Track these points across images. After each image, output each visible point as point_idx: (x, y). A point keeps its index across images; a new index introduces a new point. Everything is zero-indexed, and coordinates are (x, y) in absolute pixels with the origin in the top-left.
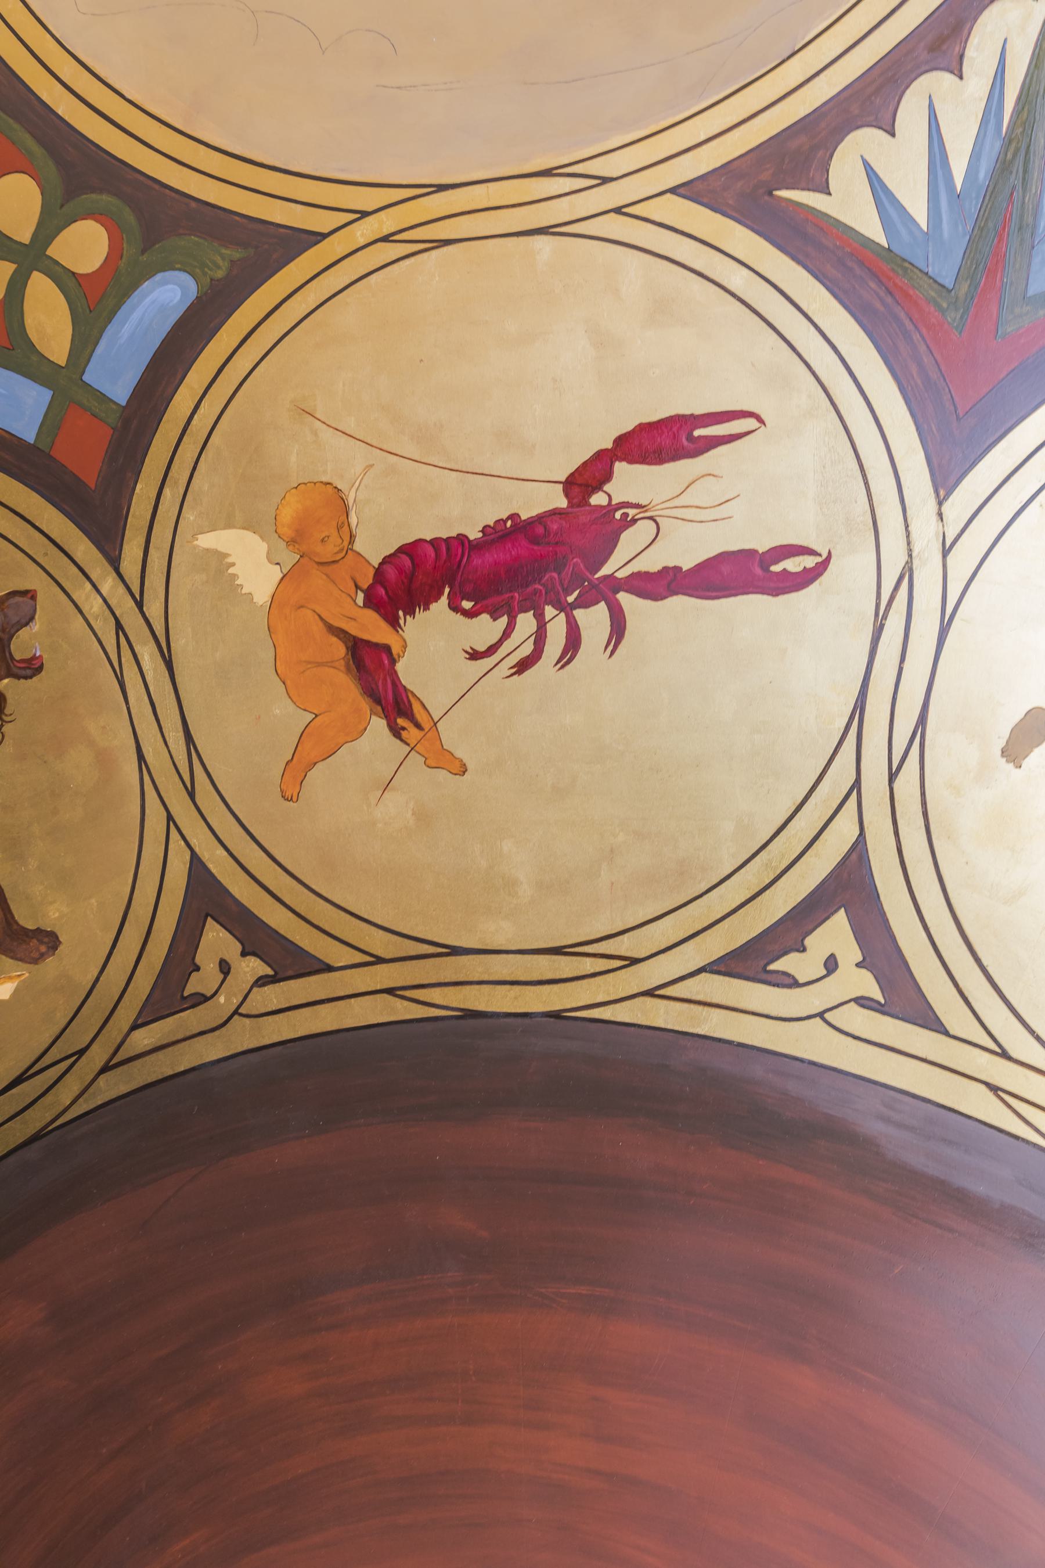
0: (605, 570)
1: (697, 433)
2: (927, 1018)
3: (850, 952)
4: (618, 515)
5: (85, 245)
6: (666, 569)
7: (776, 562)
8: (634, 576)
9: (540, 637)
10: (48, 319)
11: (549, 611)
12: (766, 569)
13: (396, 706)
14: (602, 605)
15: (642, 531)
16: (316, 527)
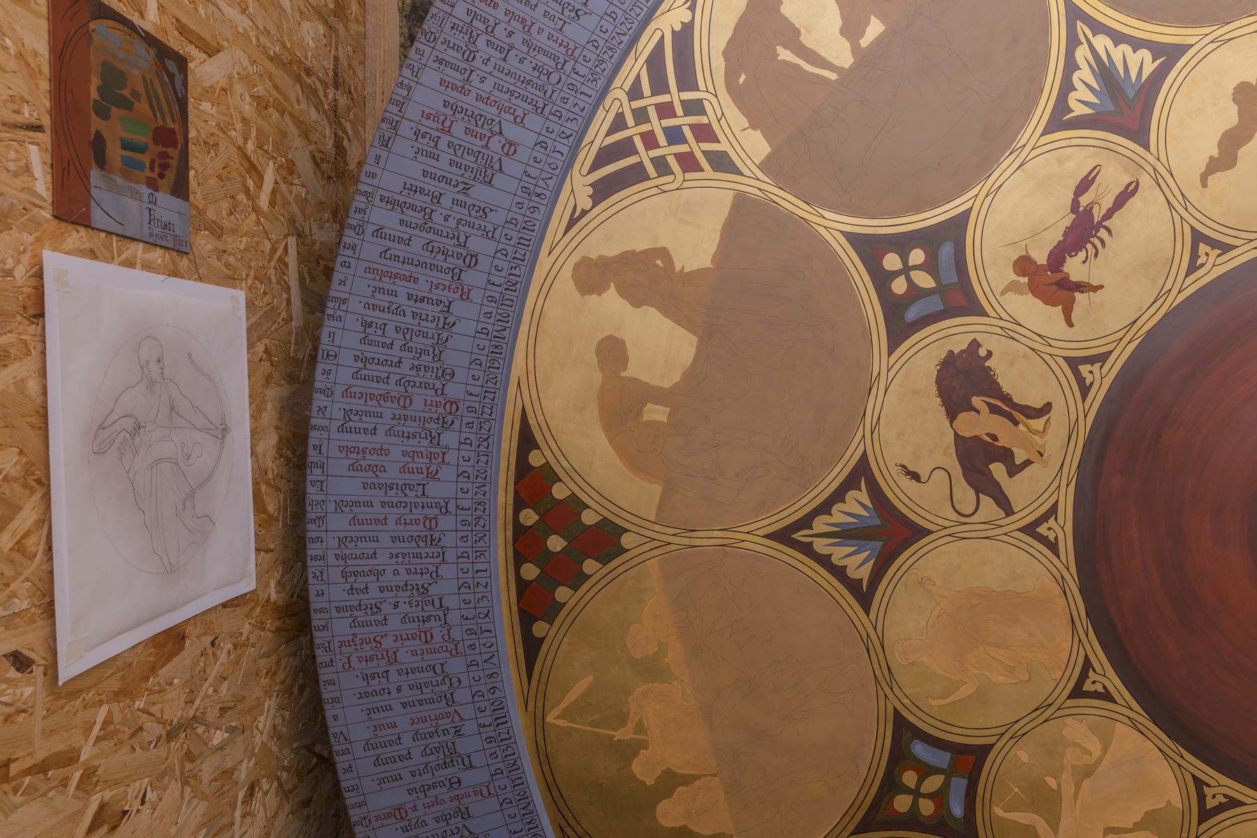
5: (917, 256)
9: (1094, 246)
10: (924, 280)
13: (1081, 287)
15: (1096, 207)
16: (1024, 265)
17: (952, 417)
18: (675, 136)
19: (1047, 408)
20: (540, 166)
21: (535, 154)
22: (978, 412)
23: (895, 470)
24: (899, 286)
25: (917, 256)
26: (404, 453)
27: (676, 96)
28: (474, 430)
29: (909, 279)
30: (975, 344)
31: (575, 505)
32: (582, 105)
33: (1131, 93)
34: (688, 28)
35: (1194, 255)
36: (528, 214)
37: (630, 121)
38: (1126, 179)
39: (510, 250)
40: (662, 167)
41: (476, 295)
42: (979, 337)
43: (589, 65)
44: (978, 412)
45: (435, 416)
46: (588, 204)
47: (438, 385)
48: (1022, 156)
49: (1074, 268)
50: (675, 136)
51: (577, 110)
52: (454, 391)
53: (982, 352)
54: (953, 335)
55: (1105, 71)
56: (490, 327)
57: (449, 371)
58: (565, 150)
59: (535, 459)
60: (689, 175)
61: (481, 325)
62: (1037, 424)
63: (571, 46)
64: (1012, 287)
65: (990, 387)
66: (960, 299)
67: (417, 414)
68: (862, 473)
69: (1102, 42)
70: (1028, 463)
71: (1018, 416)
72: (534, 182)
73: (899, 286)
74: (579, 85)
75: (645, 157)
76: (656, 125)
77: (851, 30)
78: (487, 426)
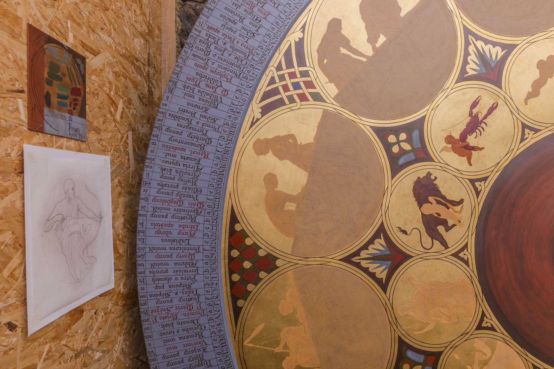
5: (403, 136)
9: (480, 131)
10: (406, 147)
13: (474, 148)
16: (449, 139)
17: (420, 206)
18: (297, 86)
19: (462, 201)
20: (238, 100)
21: (236, 95)
22: (431, 203)
23: (396, 230)
24: (395, 149)
25: (403, 136)
26: (180, 226)
27: (297, 69)
28: (211, 215)
29: (399, 146)
30: (429, 174)
31: (255, 247)
32: (256, 73)
33: (493, 65)
34: (301, 40)
35: (523, 134)
36: (233, 121)
37: (277, 80)
38: (492, 102)
39: (226, 136)
40: (291, 99)
41: (211, 156)
42: (431, 171)
43: (259, 56)
44: (431, 203)
45: (193, 209)
46: (259, 116)
47: (195, 196)
48: (447, 92)
49: (471, 140)
50: (297, 86)
51: (254, 76)
52: (202, 198)
53: (433, 177)
54: (419, 170)
55: (481, 56)
56: (217, 170)
57: (199, 190)
58: (249, 93)
59: (238, 227)
60: (303, 103)
61: (213, 169)
62: (458, 208)
63: (251, 48)
64: (445, 149)
65: (436, 192)
66: (422, 154)
67: (186, 209)
68: (381, 231)
69: (480, 44)
70: (454, 225)
71: (449, 205)
72: (236, 107)
73: (395, 149)
74: (255, 65)
75: (284, 95)
76: (289, 81)
77: (372, 40)
78: (216, 213)
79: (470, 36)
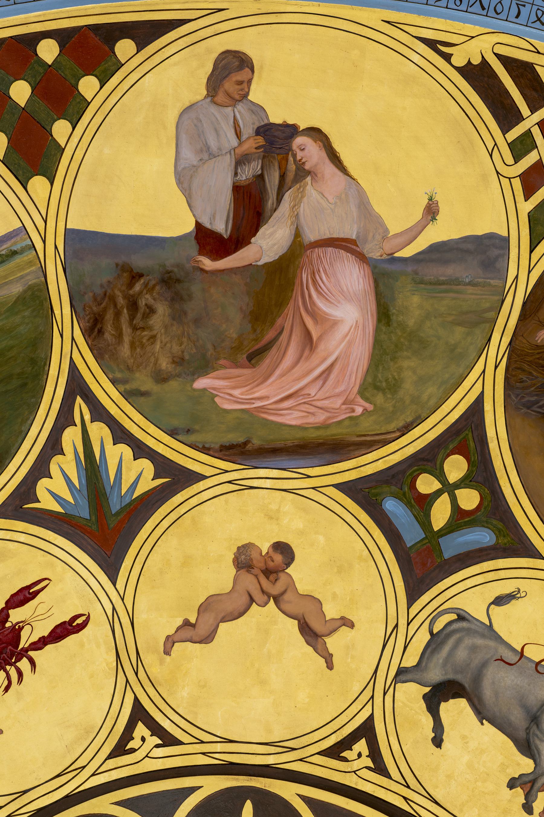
0: (21, 647)
1: (31, 591)
2: (177, 742)
3: (146, 733)
4: (17, 627)
6: (40, 638)
7: (74, 623)
8: (30, 645)
11: (8, 667)
12: (71, 625)
14: (24, 658)
33: (115, 505)
55: (92, 466)
69: (99, 432)
79: (79, 400)
